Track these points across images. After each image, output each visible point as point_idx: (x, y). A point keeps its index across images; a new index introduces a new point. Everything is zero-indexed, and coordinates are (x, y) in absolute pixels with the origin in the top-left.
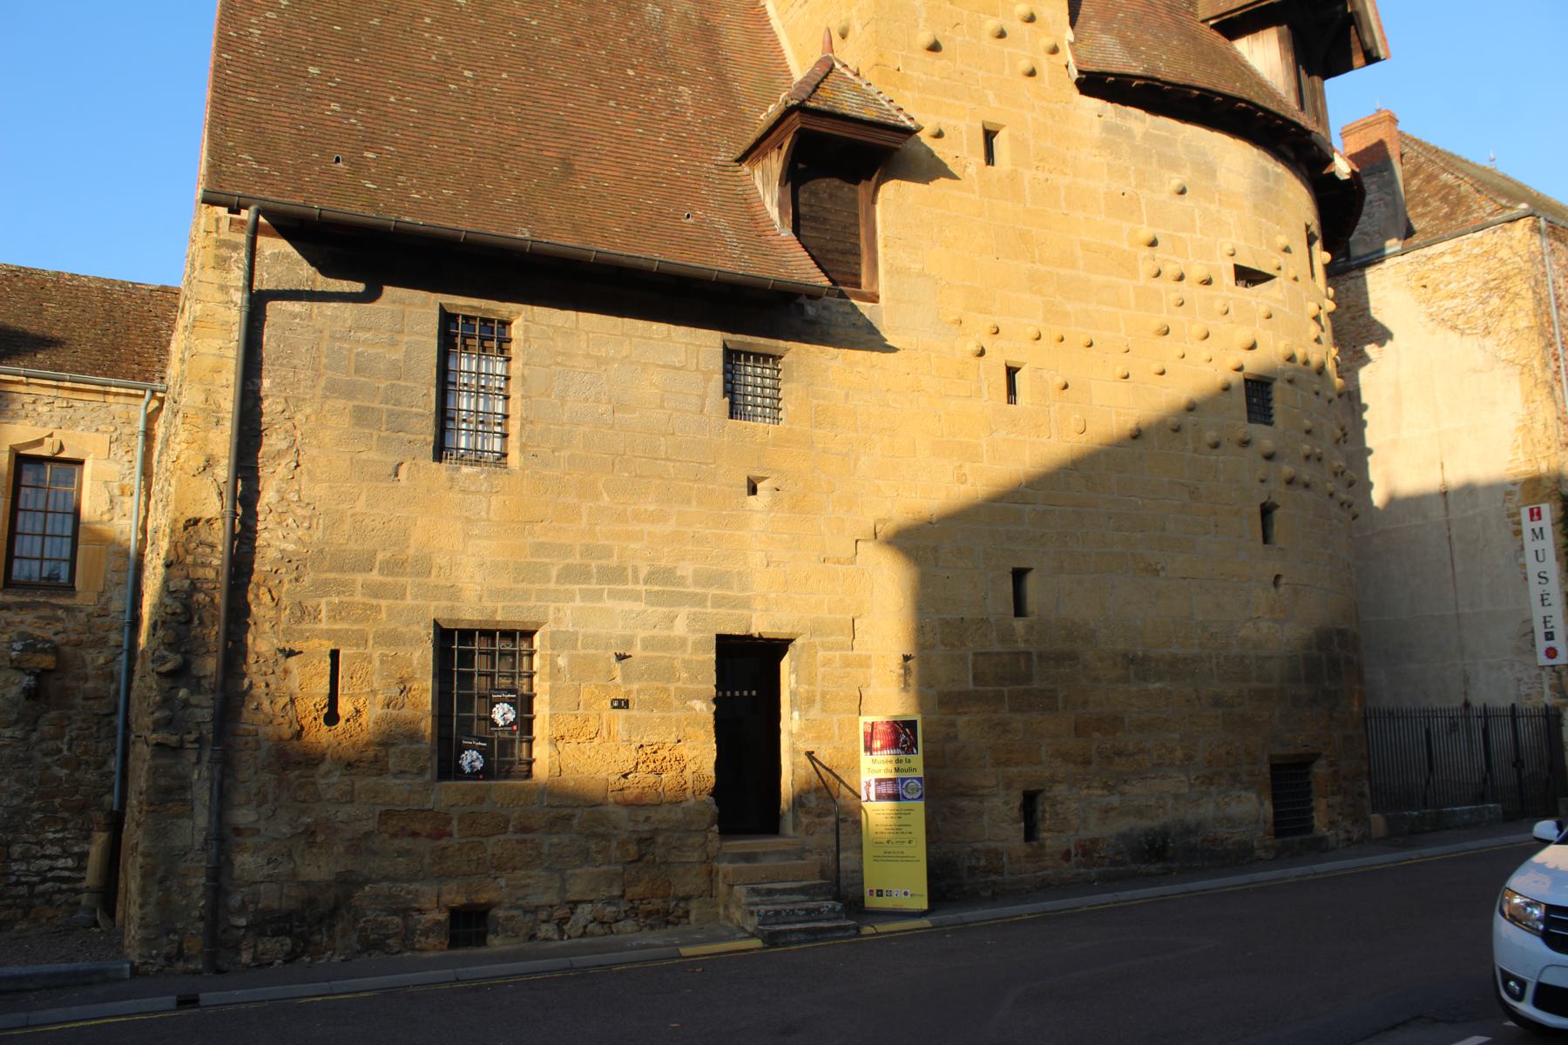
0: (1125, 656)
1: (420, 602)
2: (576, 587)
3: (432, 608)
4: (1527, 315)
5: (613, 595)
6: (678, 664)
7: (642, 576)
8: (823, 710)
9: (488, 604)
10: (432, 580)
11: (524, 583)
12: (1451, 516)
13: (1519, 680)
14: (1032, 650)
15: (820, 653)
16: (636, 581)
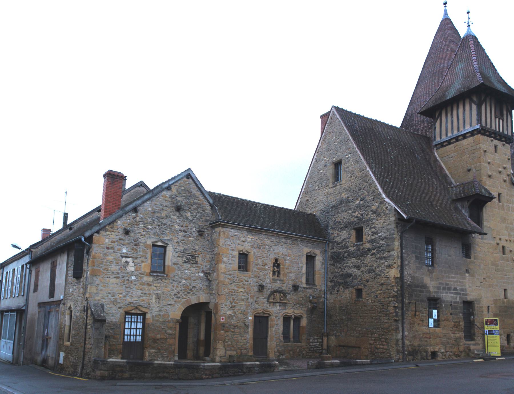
5: (450, 293)
7: (453, 289)
16: (452, 290)
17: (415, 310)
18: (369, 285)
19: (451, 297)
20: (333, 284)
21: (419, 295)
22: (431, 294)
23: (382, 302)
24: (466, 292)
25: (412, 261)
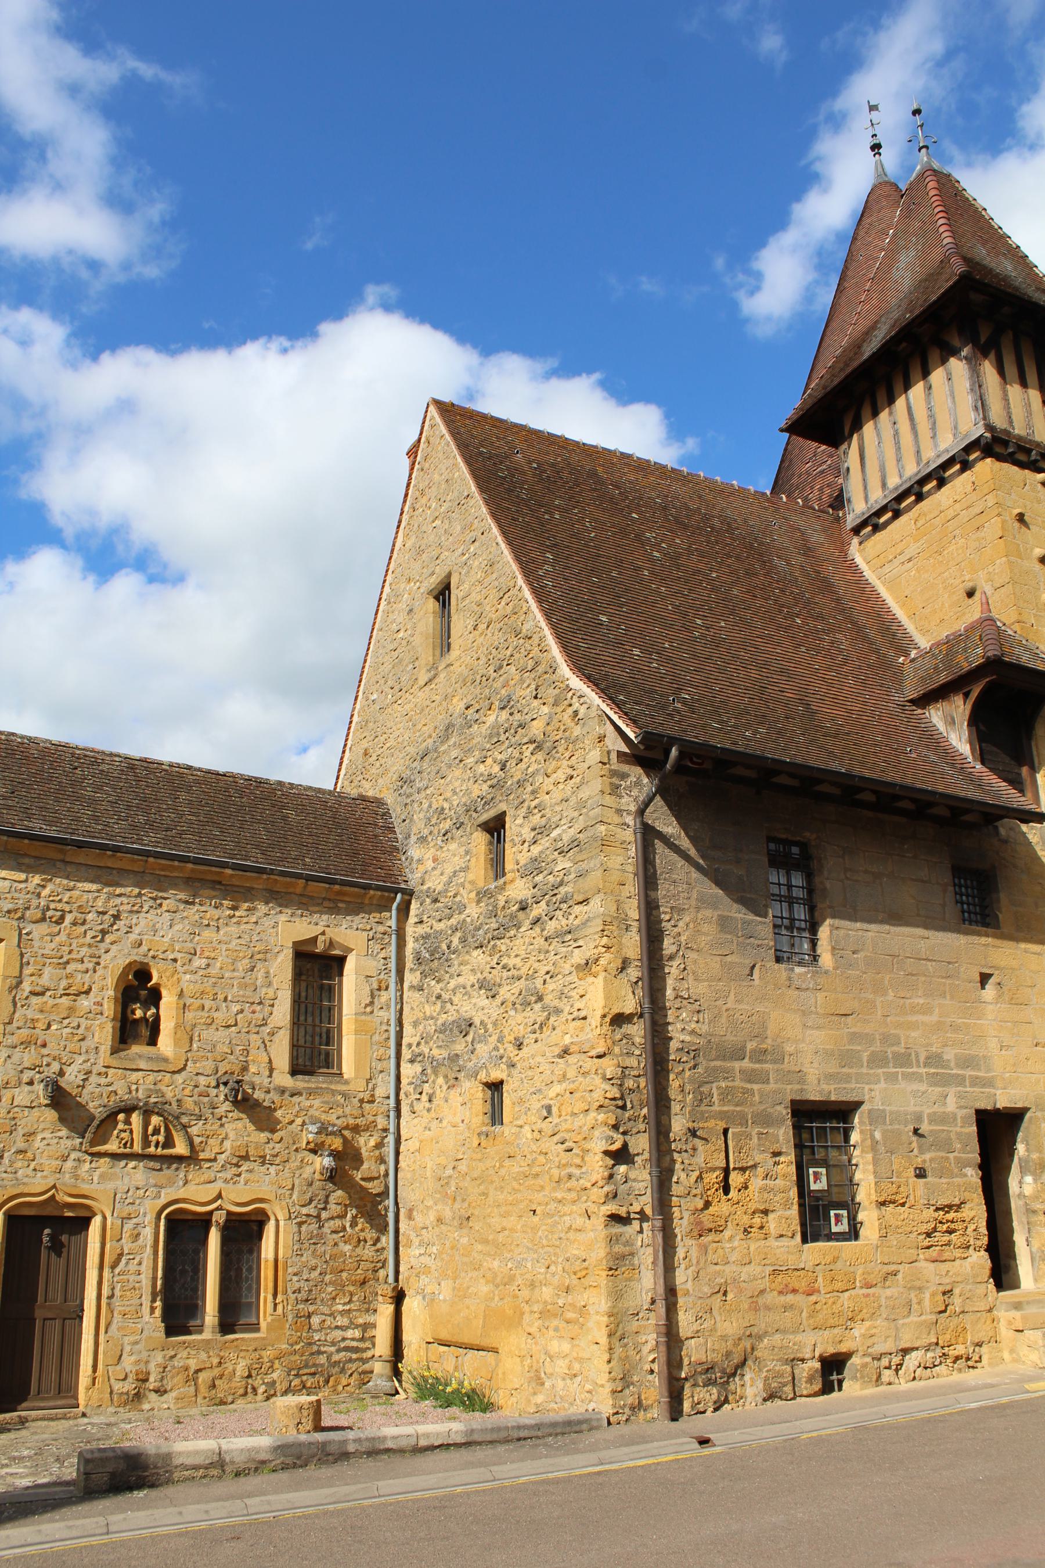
17: (723, 1164)
18: (523, 1059)
20: (418, 1068)
21: (745, 1091)
23: (567, 1136)
25: (703, 940)
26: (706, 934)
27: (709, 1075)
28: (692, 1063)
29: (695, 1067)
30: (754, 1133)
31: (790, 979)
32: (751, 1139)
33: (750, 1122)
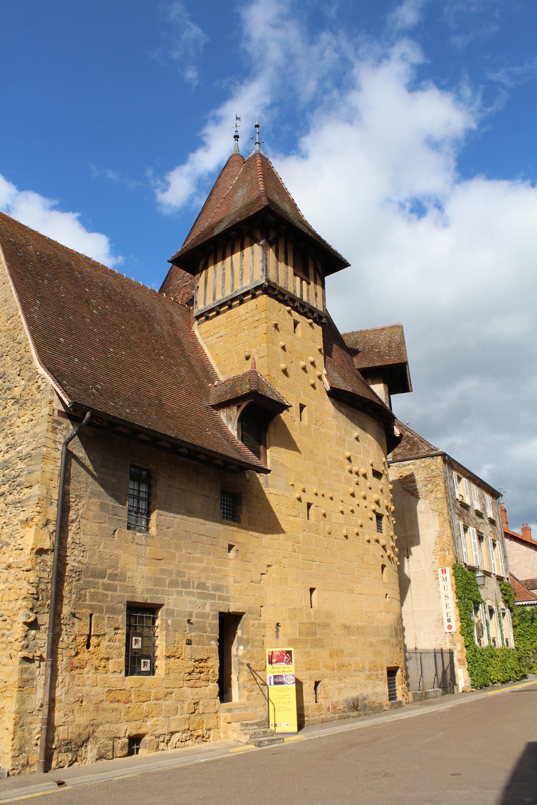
0: (344, 625)
1: (122, 593)
2: (174, 589)
3: (126, 596)
4: (441, 493)
5: (187, 593)
6: (207, 624)
7: (195, 585)
8: (252, 646)
9: (146, 596)
10: (126, 583)
11: (157, 586)
12: (410, 571)
13: (437, 638)
14: (316, 622)
15: (251, 621)
17: (88, 633)
19: (190, 602)
22: (137, 596)
24: (228, 593)
26: (93, 511)
27: (85, 585)
28: (77, 578)
29: (78, 580)
30: (106, 617)
31: (133, 538)
32: (104, 620)
33: (104, 611)
